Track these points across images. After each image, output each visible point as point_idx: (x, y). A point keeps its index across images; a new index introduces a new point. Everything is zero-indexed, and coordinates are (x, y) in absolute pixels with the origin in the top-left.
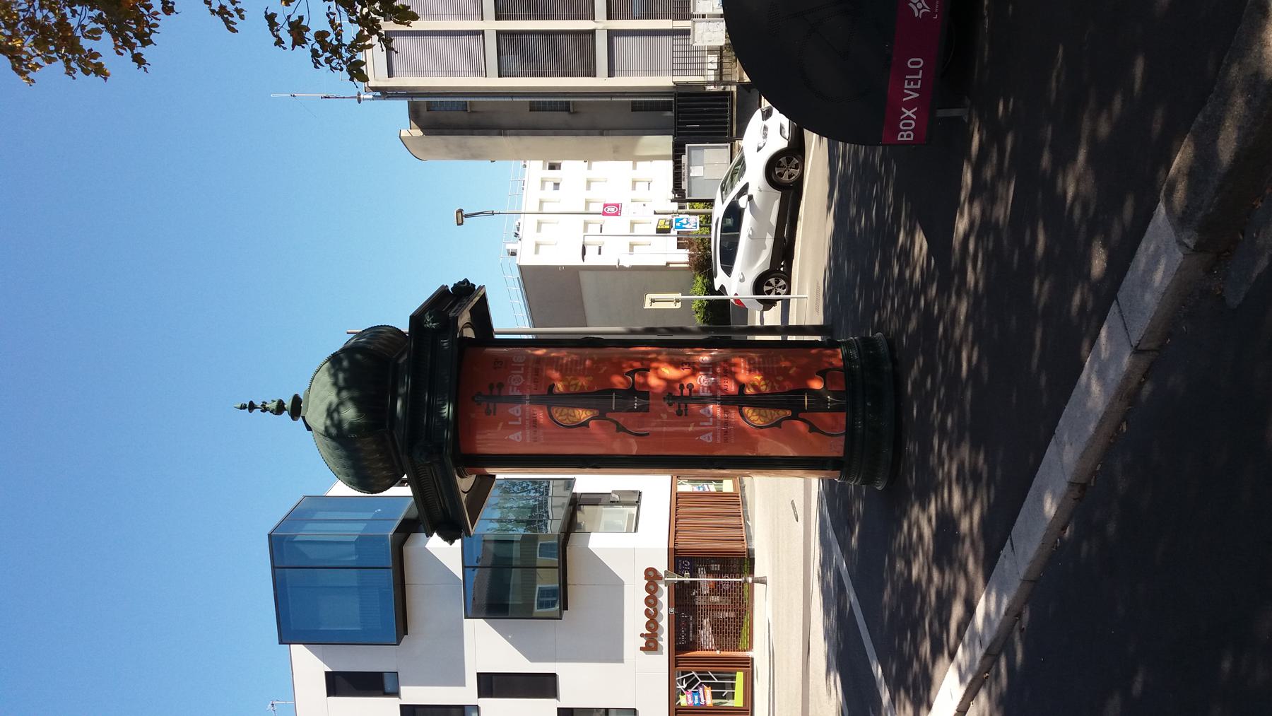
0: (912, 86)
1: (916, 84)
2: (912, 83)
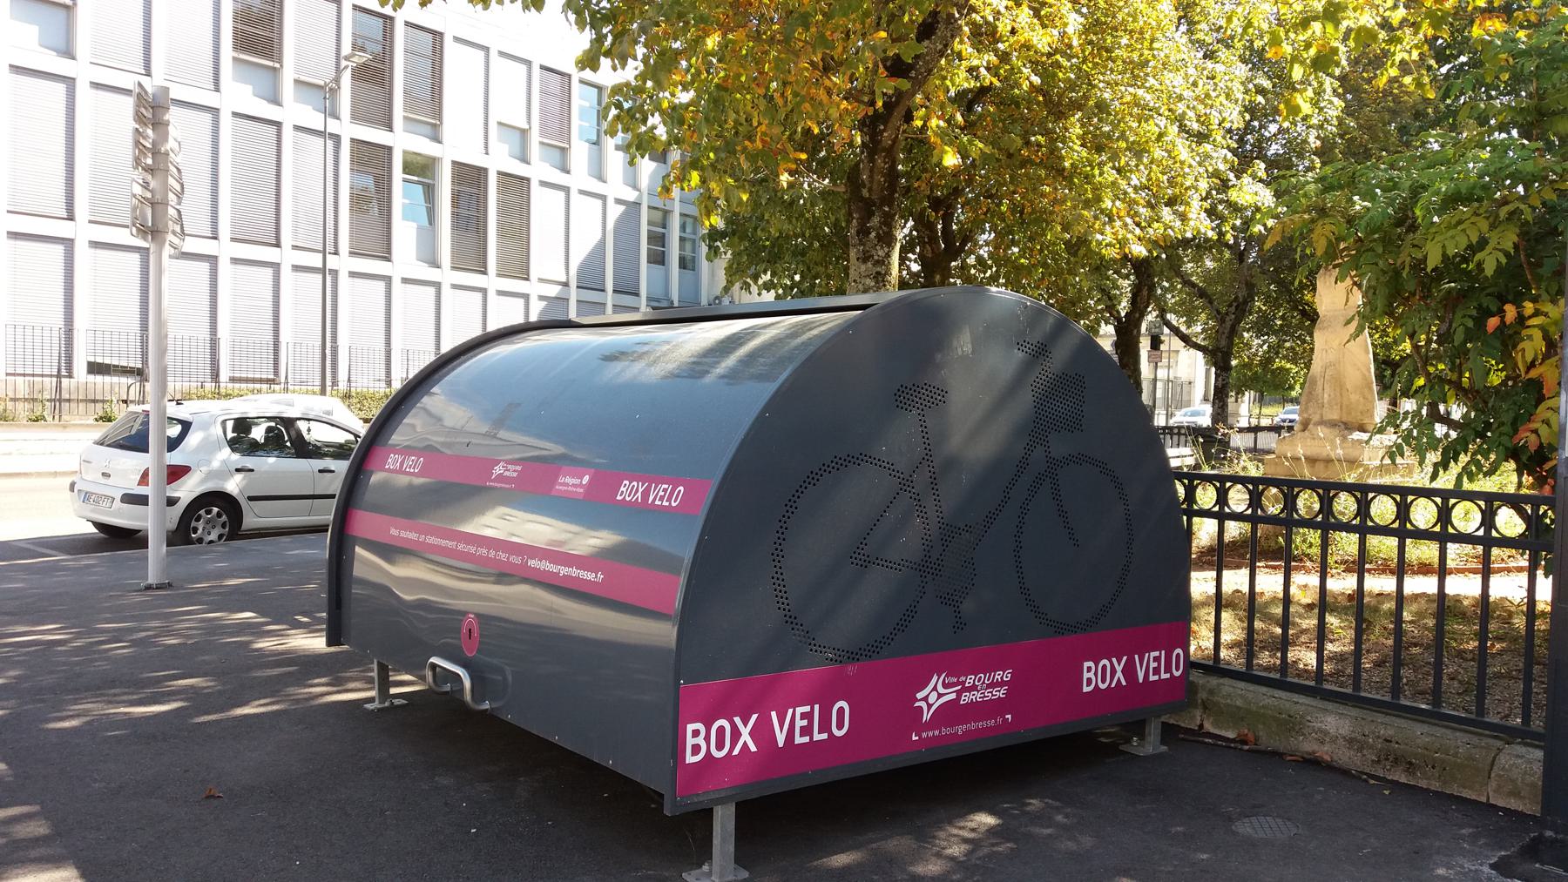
0: (800, 723)
1: (806, 731)
2: (805, 723)
